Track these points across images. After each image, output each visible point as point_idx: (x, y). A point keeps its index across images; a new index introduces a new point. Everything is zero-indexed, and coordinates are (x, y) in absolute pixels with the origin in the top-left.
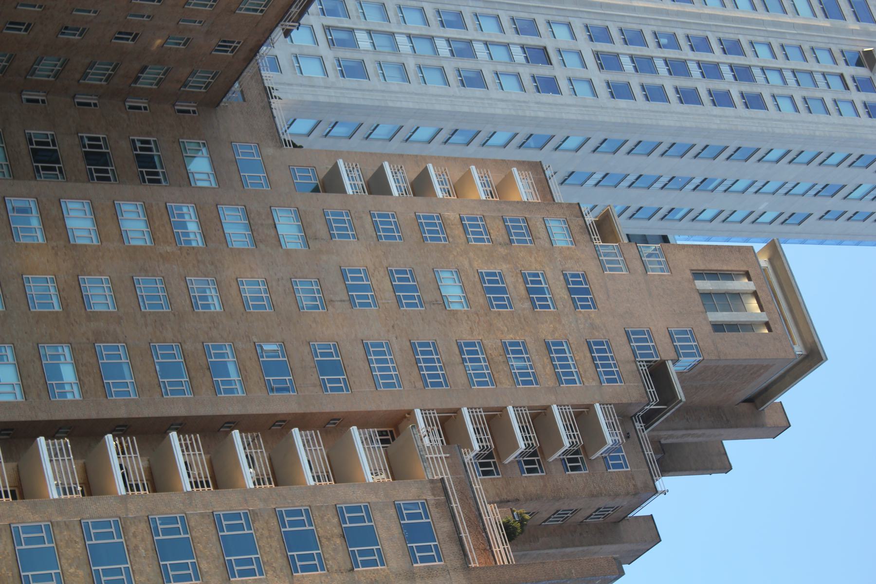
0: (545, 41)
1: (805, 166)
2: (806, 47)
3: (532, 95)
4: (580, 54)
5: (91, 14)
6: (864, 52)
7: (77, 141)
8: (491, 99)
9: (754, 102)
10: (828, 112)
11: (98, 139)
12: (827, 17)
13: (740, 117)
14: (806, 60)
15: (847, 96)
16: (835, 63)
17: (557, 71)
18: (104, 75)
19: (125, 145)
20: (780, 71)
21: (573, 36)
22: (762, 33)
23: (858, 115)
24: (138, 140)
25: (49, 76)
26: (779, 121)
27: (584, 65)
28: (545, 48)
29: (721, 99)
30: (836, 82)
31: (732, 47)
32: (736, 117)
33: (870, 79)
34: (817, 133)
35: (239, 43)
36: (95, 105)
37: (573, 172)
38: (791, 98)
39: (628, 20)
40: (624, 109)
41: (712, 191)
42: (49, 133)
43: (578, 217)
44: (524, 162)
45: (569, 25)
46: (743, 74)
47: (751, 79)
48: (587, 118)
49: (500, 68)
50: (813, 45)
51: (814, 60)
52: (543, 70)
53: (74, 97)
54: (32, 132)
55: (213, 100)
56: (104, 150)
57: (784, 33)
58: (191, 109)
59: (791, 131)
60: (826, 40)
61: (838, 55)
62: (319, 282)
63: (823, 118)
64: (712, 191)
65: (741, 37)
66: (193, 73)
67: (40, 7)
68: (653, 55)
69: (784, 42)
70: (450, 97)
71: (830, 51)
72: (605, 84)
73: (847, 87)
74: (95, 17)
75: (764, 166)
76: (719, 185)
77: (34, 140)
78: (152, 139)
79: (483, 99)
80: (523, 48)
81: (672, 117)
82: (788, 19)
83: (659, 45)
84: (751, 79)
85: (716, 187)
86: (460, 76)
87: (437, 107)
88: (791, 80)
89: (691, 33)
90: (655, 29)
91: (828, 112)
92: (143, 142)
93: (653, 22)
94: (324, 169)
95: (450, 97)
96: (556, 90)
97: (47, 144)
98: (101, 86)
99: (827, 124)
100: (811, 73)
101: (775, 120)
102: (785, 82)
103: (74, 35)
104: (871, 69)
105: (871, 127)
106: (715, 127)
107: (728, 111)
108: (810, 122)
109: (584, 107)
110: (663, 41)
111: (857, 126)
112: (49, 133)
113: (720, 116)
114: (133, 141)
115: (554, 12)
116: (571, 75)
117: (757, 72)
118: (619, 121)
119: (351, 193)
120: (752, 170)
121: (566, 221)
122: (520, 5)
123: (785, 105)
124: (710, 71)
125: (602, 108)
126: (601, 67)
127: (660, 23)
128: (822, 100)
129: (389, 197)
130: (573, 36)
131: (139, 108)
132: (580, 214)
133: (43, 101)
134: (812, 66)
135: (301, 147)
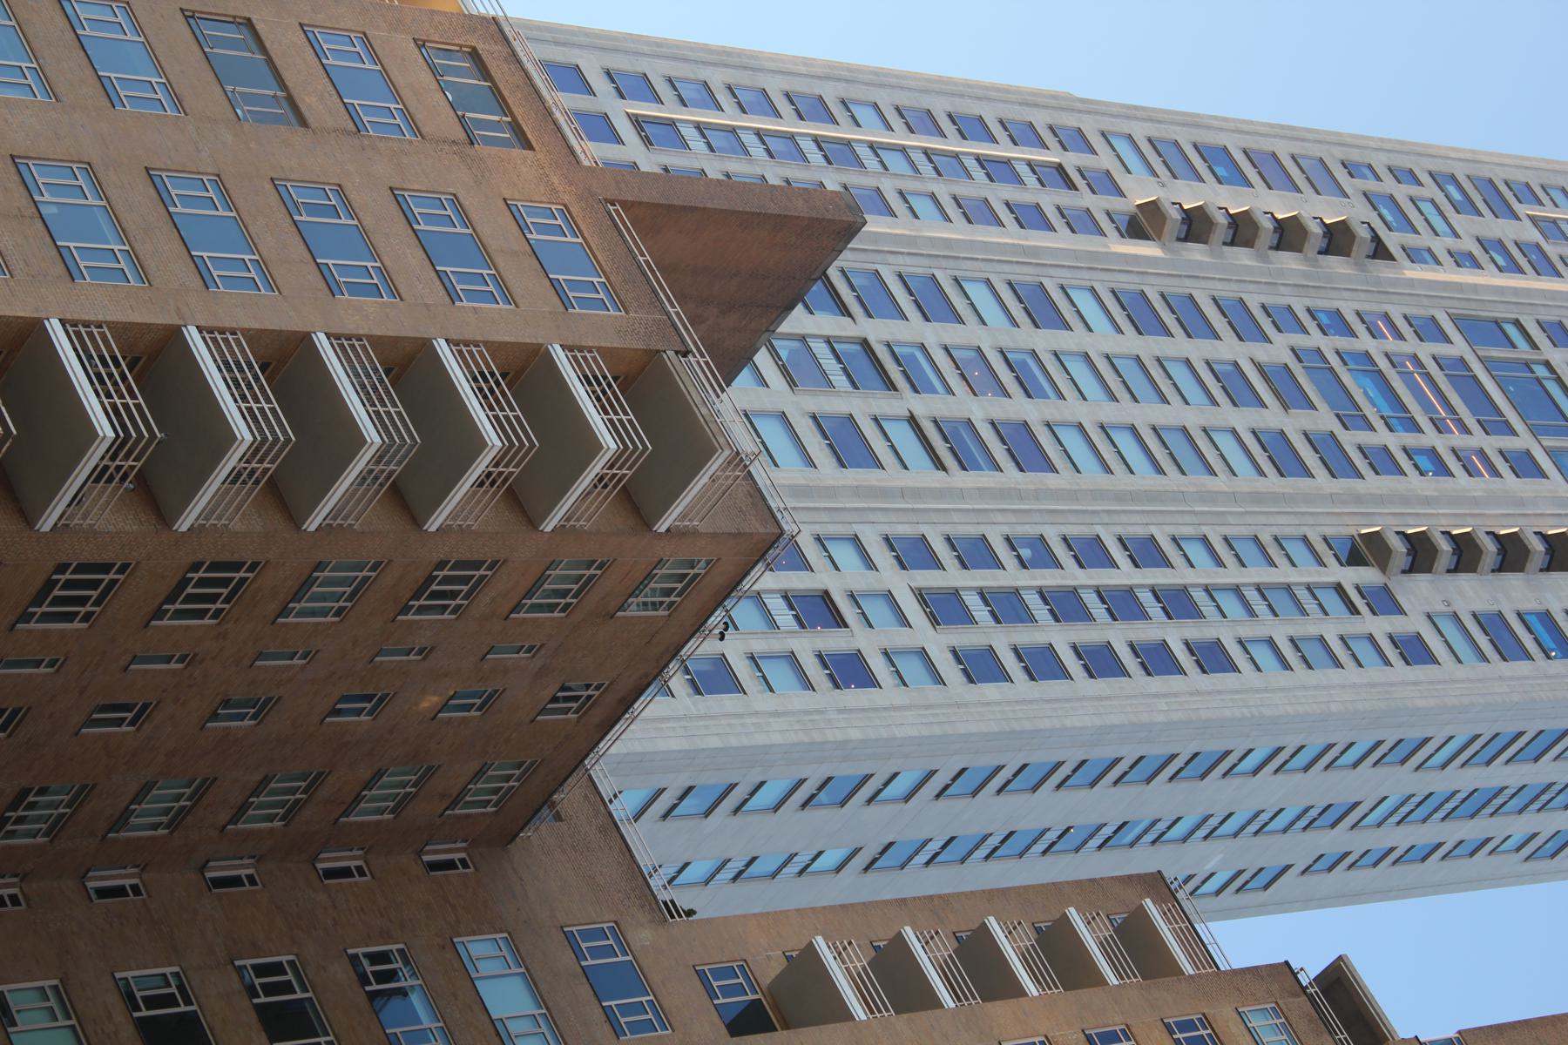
0: (820, 578)
1: (1301, 775)
2: (1266, 538)
3: (826, 696)
4: (889, 597)
5: (296, 661)
6: (1361, 535)
7: (236, 984)
8: (757, 713)
9: (1212, 658)
10: (1338, 664)
11: (277, 968)
12: (964, 469)
13: (1198, 693)
14: (1272, 563)
15: (1353, 626)
16: (1321, 563)
17: (855, 638)
18: (282, 804)
19: (341, 972)
20: (1237, 590)
21: (870, 564)
22: (1188, 519)
23: (1387, 663)
24: (366, 955)
25: (155, 827)
26: (1266, 690)
27: (905, 622)
28: (826, 592)
29: (1157, 660)
30: (1331, 600)
31: (1145, 552)
32: (1191, 694)
33: (1386, 588)
34: (1334, 708)
35: (597, 688)
36: (251, 879)
37: (891, 844)
38: (1271, 642)
39: (956, 518)
40: (998, 703)
41: (1132, 845)
42: (168, 970)
43: (1297, 996)
44: (1130, 877)
45: (856, 540)
46: (1177, 603)
47: (1195, 613)
48: (937, 730)
49: (758, 646)
50: (1276, 531)
51: (1285, 561)
52: (834, 641)
53: (203, 868)
54: (129, 974)
55: (502, 832)
56: (300, 995)
57: (1223, 513)
58: (456, 856)
59: (1289, 709)
60: (1294, 520)
61: (1321, 547)
63: (1334, 675)
64: (1132, 845)
65: (1154, 531)
66: (479, 774)
67: (182, 660)
68: (1019, 583)
69: (1227, 531)
70: (678, 719)
71: (1305, 539)
72: (950, 656)
73: (1354, 610)
74: (303, 667)
75: (1233, 782)
76: (1146, 831)
77: (138, 995)
78: (394, 947)
79: (741, 716)
80: (786, 597)
81: (1081, 711)
82: (1221, 482)
83: (1023, 564)
84: (1195, 613)
85: (1139, 837)
86: (687, 672)
87: (662, 745)
88: (1260, 607)
89: (1072, 531)
90: (1007, 530)
91: (1338, 664)
92: (376, 958)
93: (999, 518)
94: (769, 968)
95: (678, 719)
96: (867, 679)
97: (169, 1000)
98: (272, 830)
99: (1343, 687)
100: (1288, 588)
101: (1258, 691)
102: (1252, 613)
103: (242, 717)
104: (1383, 568)
105: (1415, 684)
106: (1161, 718)
107: (1173, 682)
108: (1316, 688)
109: (928, 707)
110: (1026, 553)
111: (1392, 685)
112: (168, 970)
113: (1165, 695)
114: (354, 959)
115: (824, 517)
116: (887, 644)
117: (1199, 597)
118: (995, 728)
119: (863, 1017)
120: (1215, 794)
121: (1278, 1011)
122: (826, 509)
123: (1263, 655)
124: (1122, 604)
125: (959, 705)
126: (934, 621)
127: (1012, 518)
128: (1322, 639)
129: (938, 1012)
130: (870, 564)
131: (345, 873)
132: (1298, 989)
133: (135, 889)
134: (1283, 574)
135: (690, 913)
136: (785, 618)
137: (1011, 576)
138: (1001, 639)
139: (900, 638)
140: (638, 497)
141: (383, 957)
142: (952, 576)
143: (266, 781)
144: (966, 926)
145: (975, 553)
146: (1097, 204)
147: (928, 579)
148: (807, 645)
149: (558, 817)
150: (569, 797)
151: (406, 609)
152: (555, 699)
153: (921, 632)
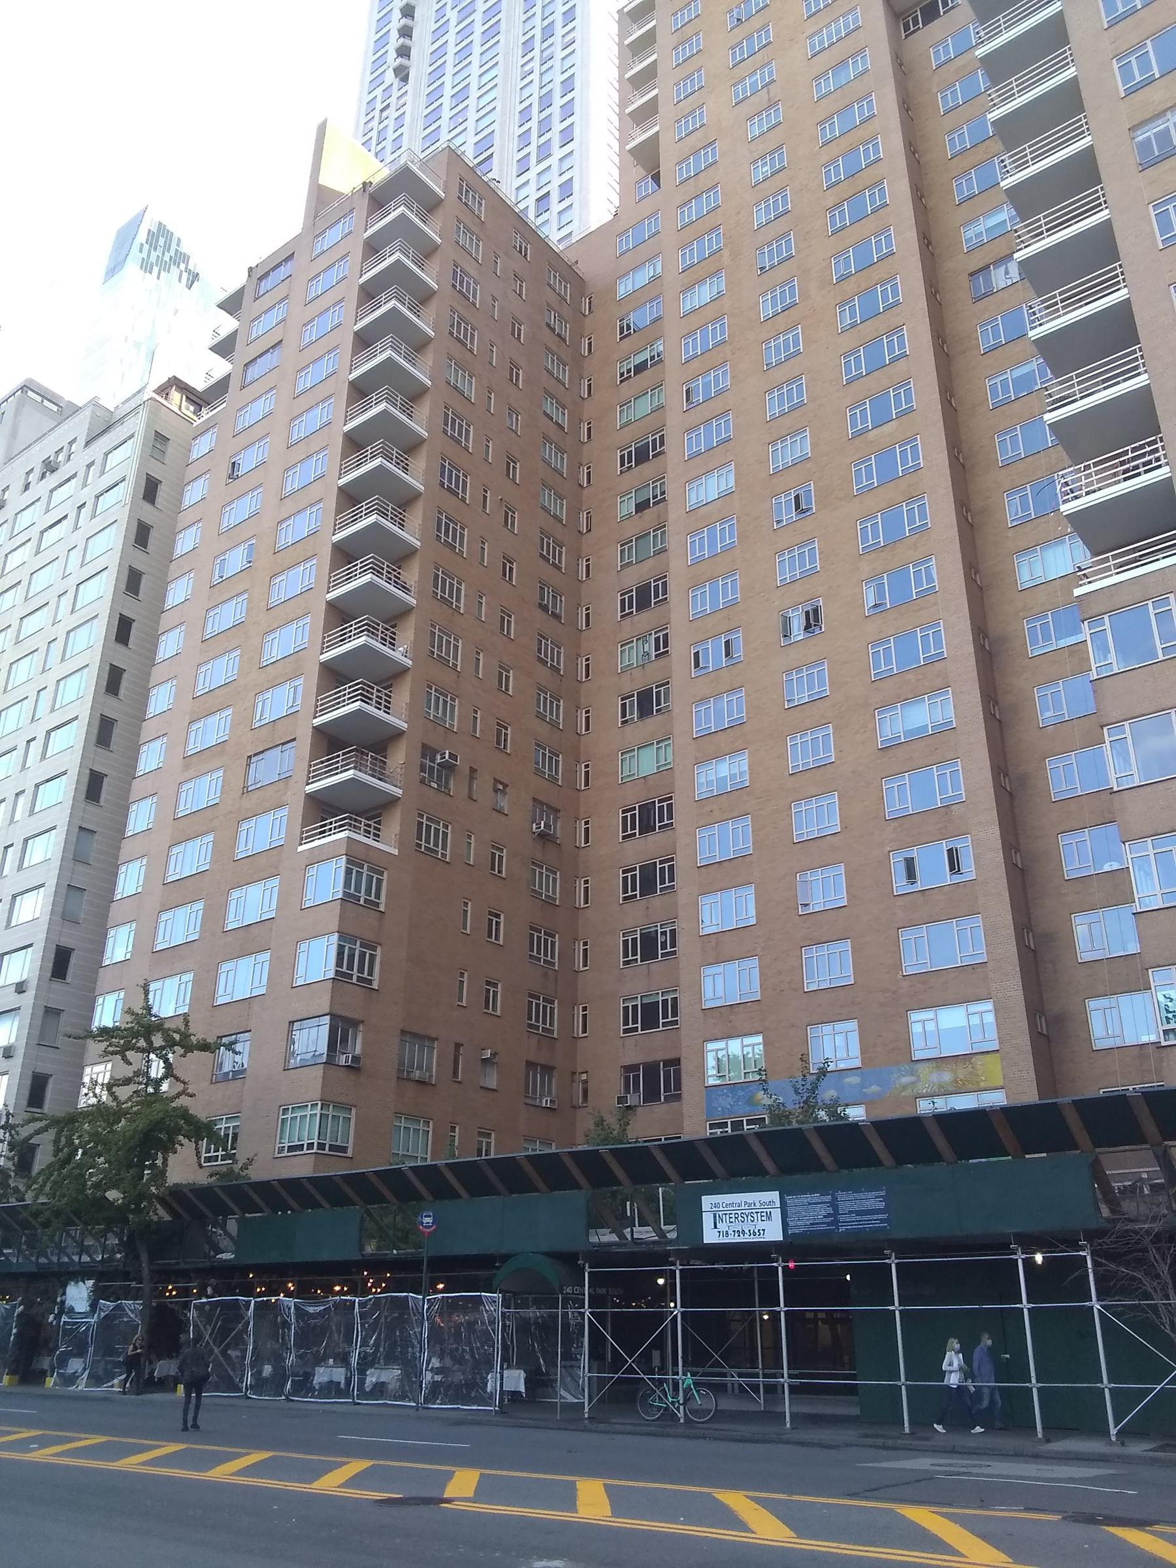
55: (578, 283)
62: (750, 119)
92: (622, 332)
94: (640, 172)
114: (621, 339)
136: (545, 216)
137: (533, 124)
138: (557, 127)
139: (555, 169)
140: (430, 205)
141: (622, 329)
142: (533, 149)
143: (548, 370)
144: (629, 87)
145: (525, 139)
146: (396, 94)
147: (533, 159)
148: (556, 207)
149: (577, 262)
150: (570, 257)
151: (474, 304)
152: (520, 252)
153: (553, 161)
